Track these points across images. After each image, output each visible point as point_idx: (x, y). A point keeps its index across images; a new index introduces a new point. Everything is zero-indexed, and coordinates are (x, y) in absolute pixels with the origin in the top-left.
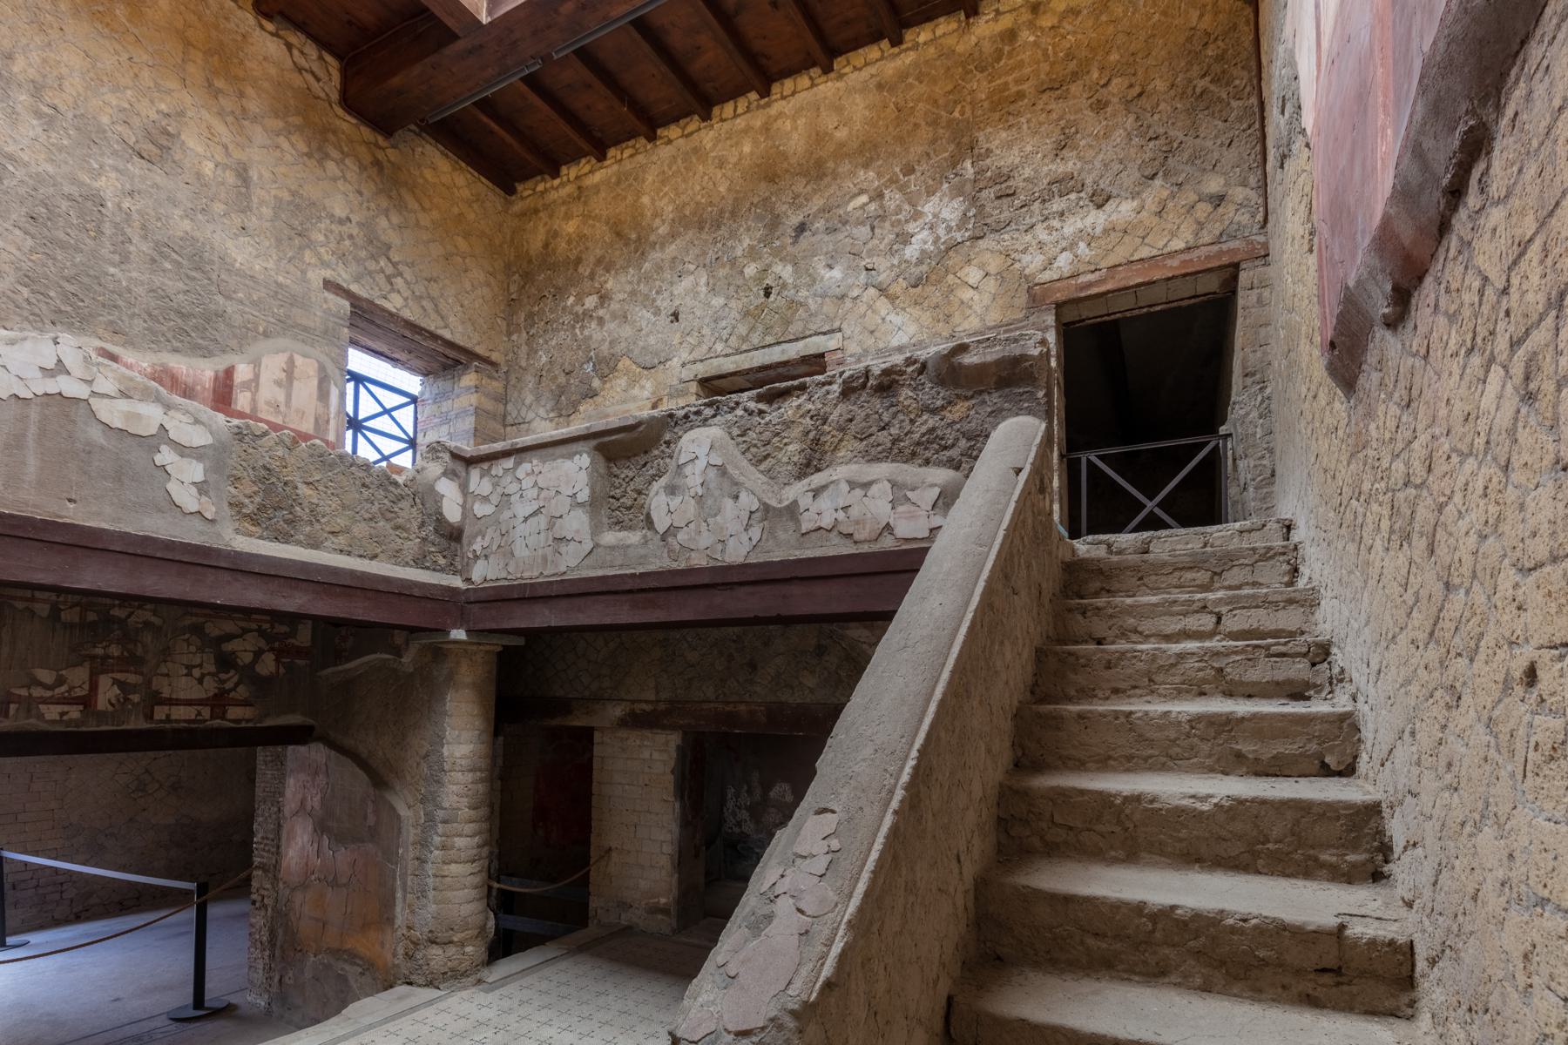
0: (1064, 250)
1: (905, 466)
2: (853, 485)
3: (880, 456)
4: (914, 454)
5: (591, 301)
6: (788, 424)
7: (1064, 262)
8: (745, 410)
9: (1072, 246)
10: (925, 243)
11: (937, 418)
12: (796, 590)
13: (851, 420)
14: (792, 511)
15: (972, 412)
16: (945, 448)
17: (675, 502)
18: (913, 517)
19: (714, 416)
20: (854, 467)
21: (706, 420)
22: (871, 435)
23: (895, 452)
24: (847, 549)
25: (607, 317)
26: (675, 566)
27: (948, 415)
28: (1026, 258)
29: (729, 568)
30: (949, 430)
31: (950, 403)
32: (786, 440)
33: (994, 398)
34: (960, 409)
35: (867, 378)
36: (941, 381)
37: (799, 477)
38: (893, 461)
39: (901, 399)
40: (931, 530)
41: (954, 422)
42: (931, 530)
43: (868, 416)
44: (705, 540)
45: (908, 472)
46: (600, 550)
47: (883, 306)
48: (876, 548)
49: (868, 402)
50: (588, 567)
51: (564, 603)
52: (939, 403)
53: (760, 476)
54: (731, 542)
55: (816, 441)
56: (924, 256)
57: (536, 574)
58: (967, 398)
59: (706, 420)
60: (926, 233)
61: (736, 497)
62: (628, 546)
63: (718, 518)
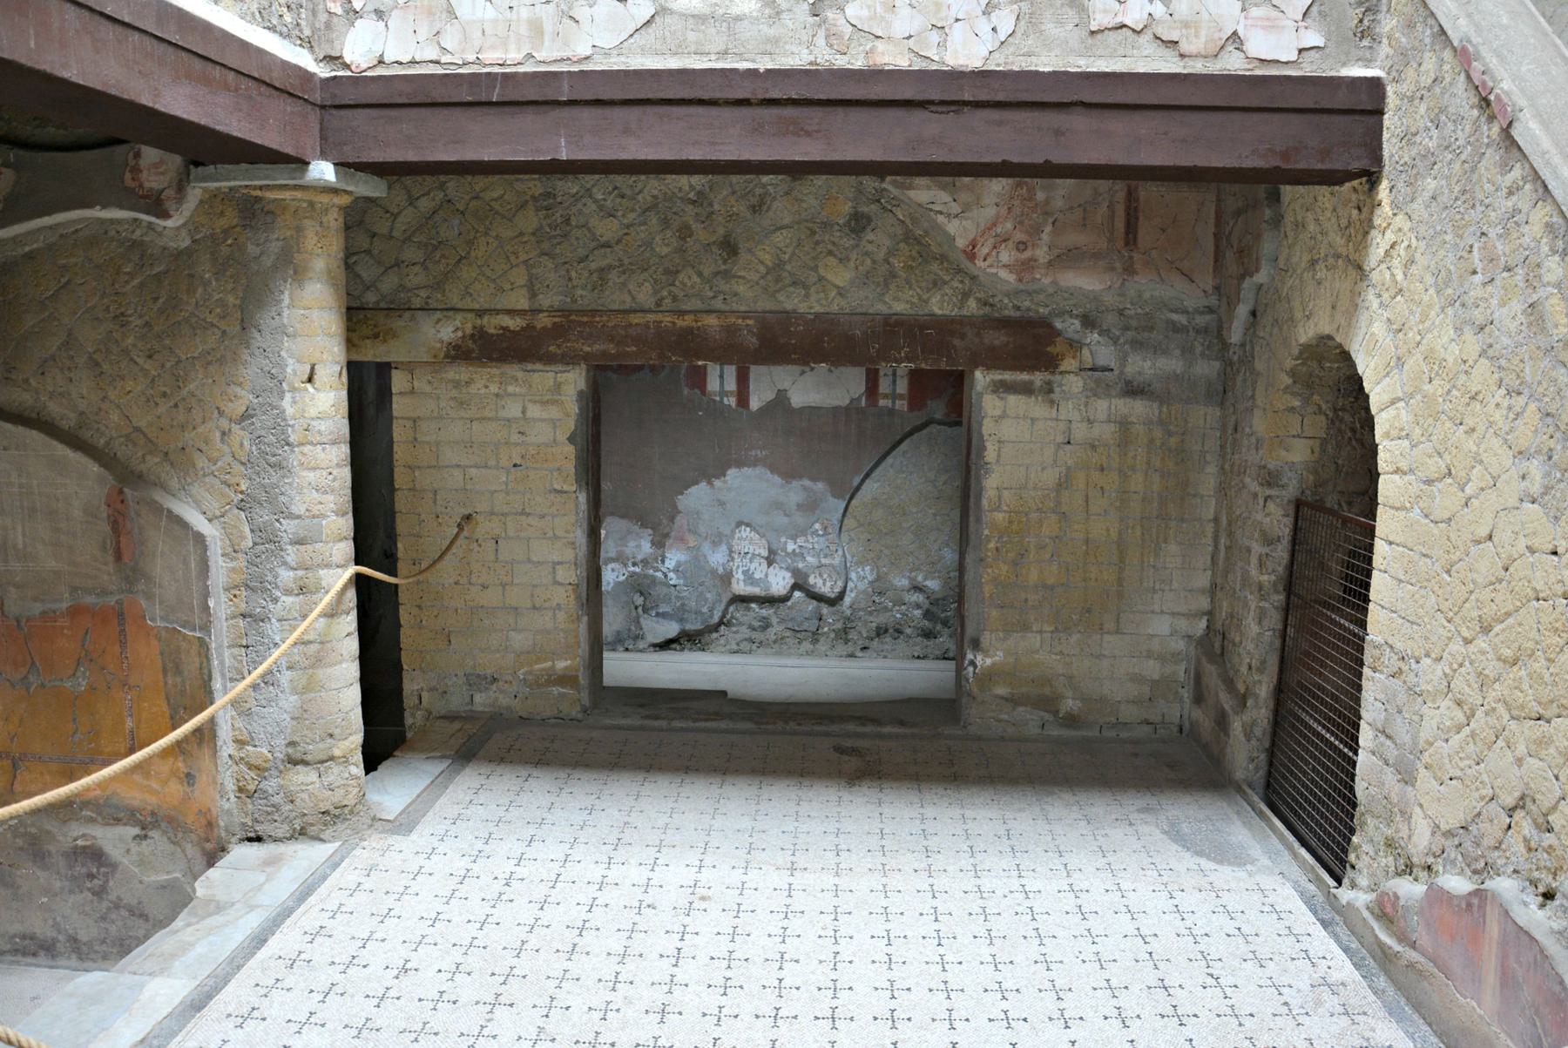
12: (1077, 122)
18: (1271, 27)
24: (1167, 64)
26: (841, 62)
29: (956, 76)
40: (1300, 51)
42: (1300, 51)
44: (904, 23)
46: (668, 19)
48: (1215, 67)
50: (643, 51)
51: (587, 115)
54: (957, 33)
57: (519, 57)
62: (738, 19)
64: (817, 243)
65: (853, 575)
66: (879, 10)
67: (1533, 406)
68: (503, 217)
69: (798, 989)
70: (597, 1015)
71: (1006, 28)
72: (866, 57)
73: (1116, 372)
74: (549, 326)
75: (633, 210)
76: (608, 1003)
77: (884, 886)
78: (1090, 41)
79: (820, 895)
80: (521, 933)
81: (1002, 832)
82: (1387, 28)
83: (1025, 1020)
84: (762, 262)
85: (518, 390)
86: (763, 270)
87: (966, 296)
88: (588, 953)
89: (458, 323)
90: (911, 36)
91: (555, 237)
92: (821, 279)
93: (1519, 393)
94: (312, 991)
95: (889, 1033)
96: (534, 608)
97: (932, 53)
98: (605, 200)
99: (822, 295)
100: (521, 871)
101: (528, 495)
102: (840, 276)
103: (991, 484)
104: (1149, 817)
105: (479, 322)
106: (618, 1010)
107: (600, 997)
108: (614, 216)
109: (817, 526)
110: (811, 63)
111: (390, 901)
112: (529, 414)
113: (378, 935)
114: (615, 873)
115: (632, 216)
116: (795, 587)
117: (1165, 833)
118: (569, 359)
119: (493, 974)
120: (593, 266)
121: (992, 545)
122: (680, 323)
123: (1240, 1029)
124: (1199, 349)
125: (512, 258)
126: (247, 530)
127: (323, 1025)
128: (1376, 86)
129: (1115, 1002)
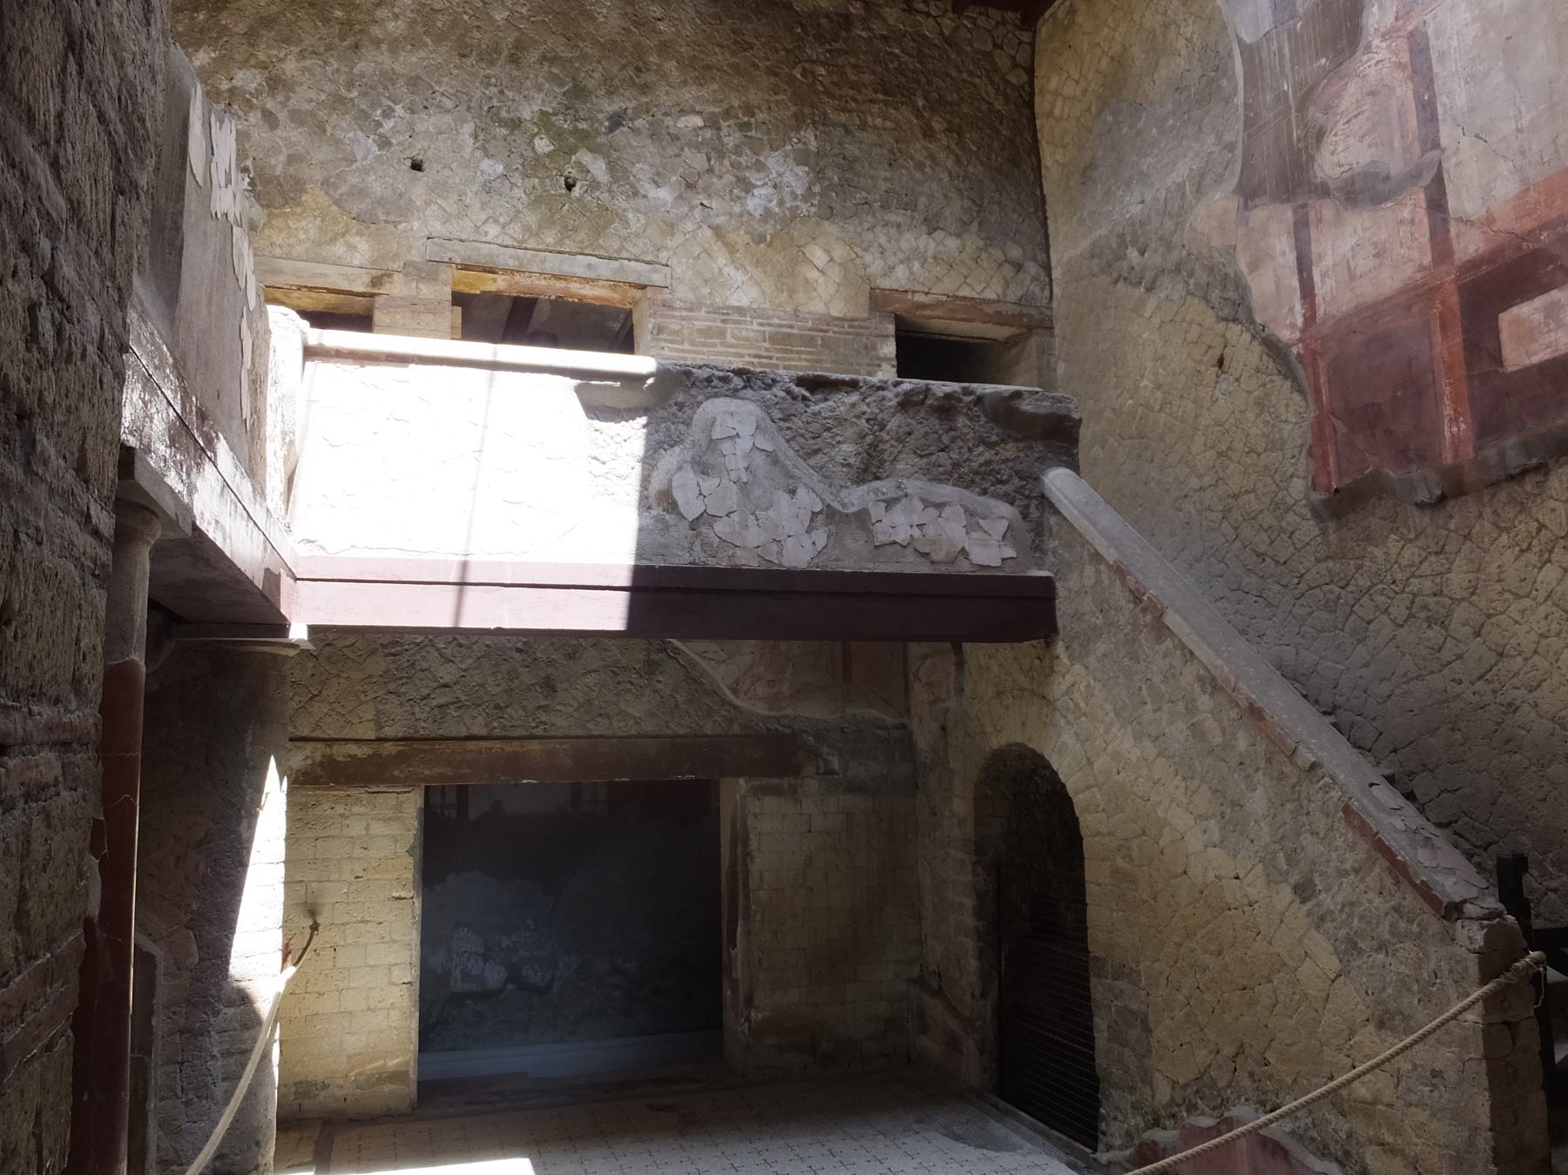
0: (901, 262)
1: (966, 492)
2: (927, 503)
3: (941, 477)
4: (973, 481)
5: (247, 79)
6: (841, 421)
7: (899, 278)
8: (788, 392)
9: (906, 261)
10: (770, 201)
11: (993, 452)
13: (910, 434)
14: (862, 518)
15: (1022, 454)
16: (1001, 482)
17: (709, 484)
18: (985, 545)
19: (744, 387)
20: (917, 482)
21: (736, 390)
22: (931, 454)
23: (957, 475)
24: (924, 568)
25: (282, 116)
26: (712, 563)
27: (1002, 451)
28: (868, 258)
29: (790, 575)
30: (1003, 467)
31: (1003, 440)
32: (839, 438)
33: (1039, 447)
34: (1010, 450)
35: (926, 397)
36: (994, 418)
37: (859, 481)
38: (954, 485)
39: (959, 425)
40: (1003, 560)
41: (1007, 460)
43: (926, 434)
44: (754, 537)
45: (971, 497)
47: (722, 259)
48: (952, 570)
49: (927, 420)
52: (994, 438)
53: (812, 471)
54: (790, 545)
55: (874, 446)
56: (767, 214)
58: (1017, 440)
59: (736, 390)
60: (769, 190)
61: (793, 492)
63: (771, 512)
64: (619, 683)
65: (561, 965)
66: (737, 527)
67: (1204, 787)
68: (354, 661)
71: (821, 542)
72: (729, 560)
73: (841, 776)
74: (393, 753)
75: (471, 657)
78: (875, 552)
82: (1051, 546)
84: (575, 698)
85: (362, 810)
86: (576, 704)
87: (731, 721)
89: (308, 752)
90: (758, 547)
91: (401, 678)
92: (622, 712)
93: (1192, 778)
96: (369, 1009)
97: (774, 559)
98: (446, 648)
99: (622, 724)
101: (367, 905)
102: (636, 710)
103: (755, 867)
105: (328, 751)
108: (453, 662)
109: (529, 921)
110: (690, 563)
112: (372, 831)
115: (470, 661)
116: (509, 980)
118: (408, 782)
120: (434, 703)
121: (758, 918)
122: (508, 748)
124: (897, 755)
125: (362, 697)
126: (195, 947)
128: (1048, 583)
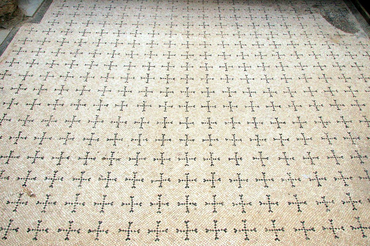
69: (194, 92)
70: (119, 108)
76: (123, 102)
77: (223, 42)
79: (199, 47)
80: (86, 69)
81: (264, 16)
83: (280, 106)
88: (113, 78)
94: (4, 103)
95: (230, 113)
100: (85, 39)
104: (317, 10)
106: (127, 105)
107: (119, 98)
111: (34, 56)
113: (30, 74)
114: (121, 38)
117: (324, 17)
119: (77, 90)
123: (361, 111)
127: (10, 120)
129: (312, 98)
